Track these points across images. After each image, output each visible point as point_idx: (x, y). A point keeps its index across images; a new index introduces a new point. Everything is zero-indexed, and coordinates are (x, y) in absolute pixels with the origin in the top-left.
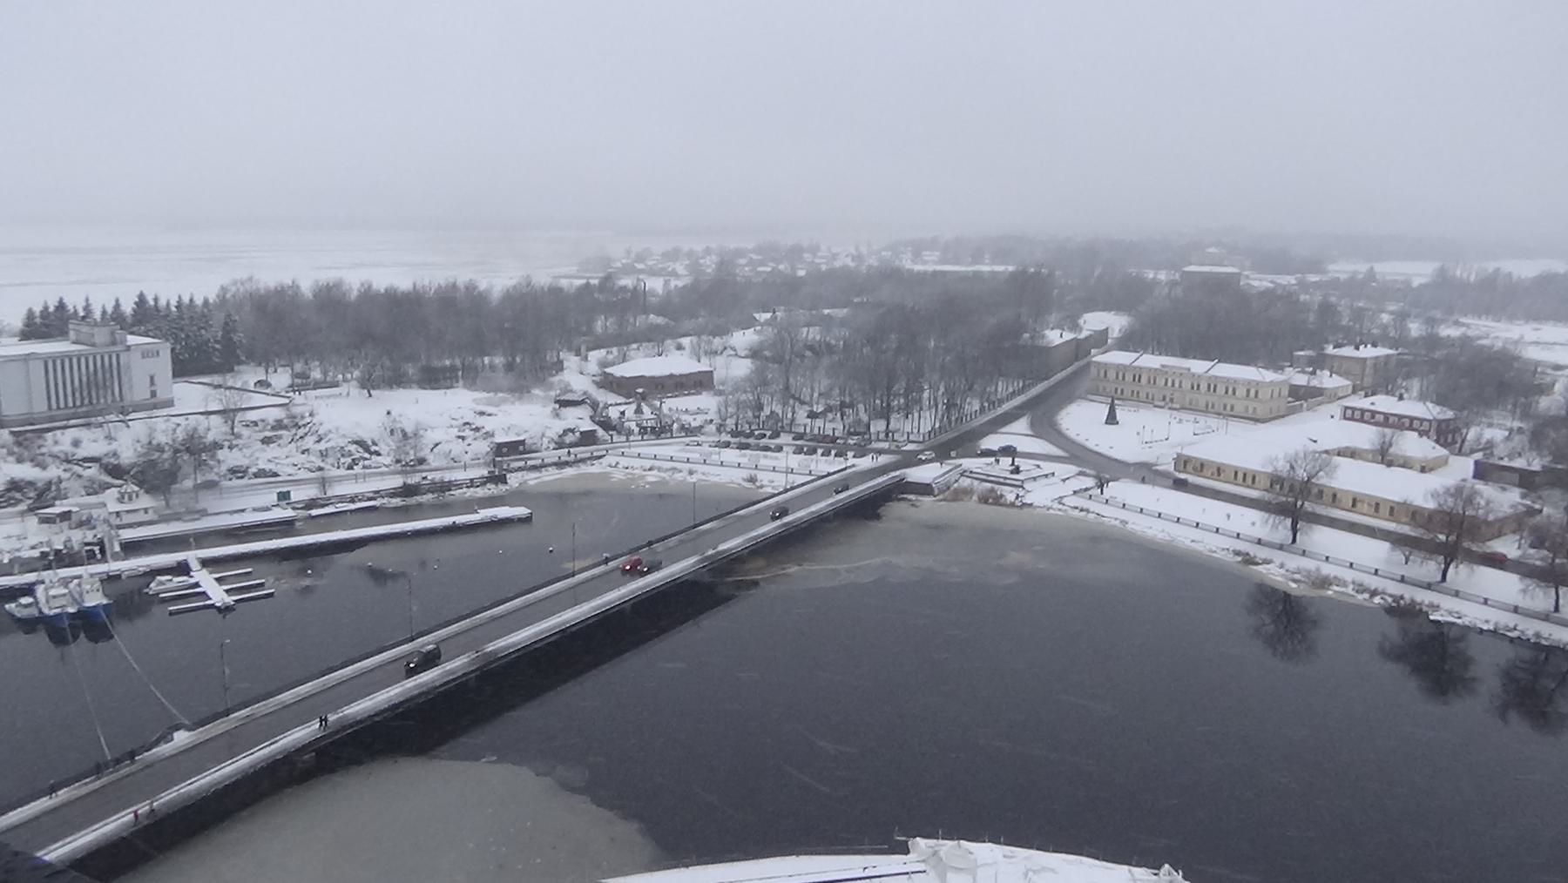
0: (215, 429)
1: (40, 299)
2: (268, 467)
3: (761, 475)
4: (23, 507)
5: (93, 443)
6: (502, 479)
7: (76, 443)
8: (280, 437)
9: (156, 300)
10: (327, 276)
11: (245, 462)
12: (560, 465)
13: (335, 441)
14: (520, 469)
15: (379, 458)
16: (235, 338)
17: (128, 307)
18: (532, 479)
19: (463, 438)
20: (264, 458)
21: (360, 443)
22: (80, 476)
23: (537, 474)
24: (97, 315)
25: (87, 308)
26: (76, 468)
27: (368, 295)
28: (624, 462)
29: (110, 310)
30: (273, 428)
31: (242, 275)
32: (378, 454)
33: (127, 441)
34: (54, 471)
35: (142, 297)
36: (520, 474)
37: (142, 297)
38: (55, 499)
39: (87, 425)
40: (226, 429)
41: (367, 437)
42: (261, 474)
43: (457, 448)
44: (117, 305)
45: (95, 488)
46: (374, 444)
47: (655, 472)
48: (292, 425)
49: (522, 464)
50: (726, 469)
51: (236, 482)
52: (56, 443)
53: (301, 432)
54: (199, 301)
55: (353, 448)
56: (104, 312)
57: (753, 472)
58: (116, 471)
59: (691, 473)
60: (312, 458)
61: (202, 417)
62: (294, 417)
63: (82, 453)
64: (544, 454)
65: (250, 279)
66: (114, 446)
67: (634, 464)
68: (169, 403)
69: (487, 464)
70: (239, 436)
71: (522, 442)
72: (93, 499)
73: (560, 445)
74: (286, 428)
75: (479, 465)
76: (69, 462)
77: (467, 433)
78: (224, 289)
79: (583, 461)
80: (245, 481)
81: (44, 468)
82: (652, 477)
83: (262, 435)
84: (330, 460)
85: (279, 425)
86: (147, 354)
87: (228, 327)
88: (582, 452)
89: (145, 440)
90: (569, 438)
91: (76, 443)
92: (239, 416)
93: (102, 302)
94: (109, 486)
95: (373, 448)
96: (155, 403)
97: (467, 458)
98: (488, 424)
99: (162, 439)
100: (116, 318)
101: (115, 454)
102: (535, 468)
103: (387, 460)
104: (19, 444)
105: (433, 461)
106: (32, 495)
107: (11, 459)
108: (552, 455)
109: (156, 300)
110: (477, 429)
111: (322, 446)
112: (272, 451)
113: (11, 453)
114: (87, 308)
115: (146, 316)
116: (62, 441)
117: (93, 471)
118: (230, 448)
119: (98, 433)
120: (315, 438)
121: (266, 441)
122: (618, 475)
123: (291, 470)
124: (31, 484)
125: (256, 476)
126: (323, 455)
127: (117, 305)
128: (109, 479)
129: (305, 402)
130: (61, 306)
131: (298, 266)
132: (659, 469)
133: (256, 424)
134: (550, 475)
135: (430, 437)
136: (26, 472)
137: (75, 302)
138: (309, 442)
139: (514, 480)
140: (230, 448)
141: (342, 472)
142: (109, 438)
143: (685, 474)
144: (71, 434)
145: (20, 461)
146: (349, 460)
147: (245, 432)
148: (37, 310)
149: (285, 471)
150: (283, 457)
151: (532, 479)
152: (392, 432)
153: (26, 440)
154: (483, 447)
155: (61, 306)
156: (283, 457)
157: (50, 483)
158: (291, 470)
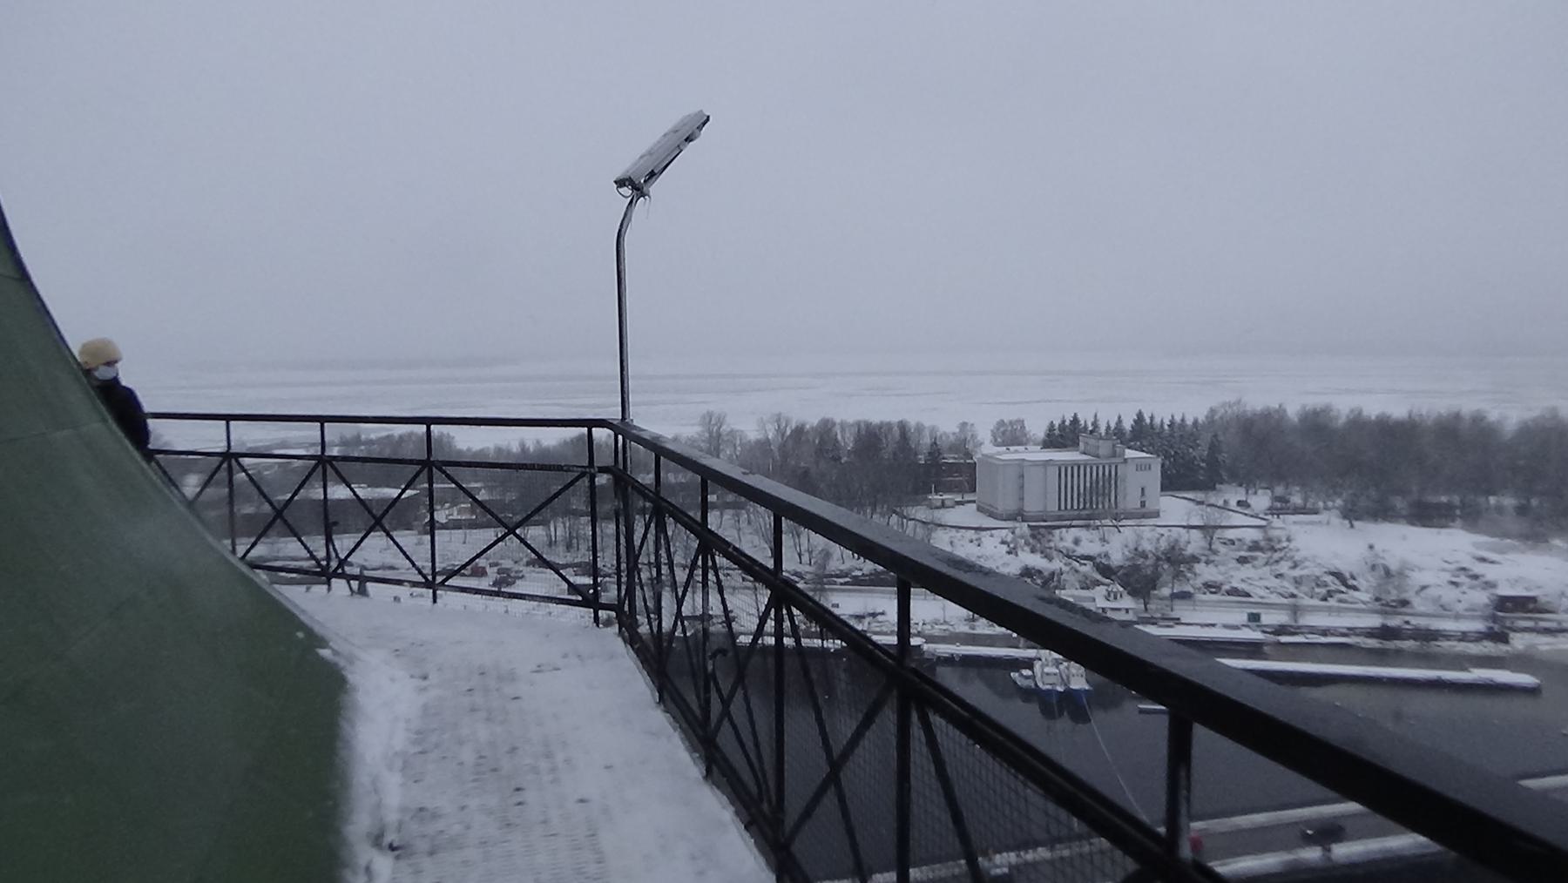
0: (1194, 543)
1: (1060, 414)
5: (1090, 543)
7: (1077, 542)
8: (1255, 558)
9: (1152, 418)
10: (1315, 402)
11: (1220, 578)
15: (1356, 594)
16: (1220, 458)
17: (1128, 424)
20: (1239, 577)
21: (1338, 575)
24: (1103, 430)
25: (1095, 424)
27: (1357, 423)
29: (1113, 425)
30: (1250, 549)
31: (1232, 398)
32: (1355, 588)
33: (1117, 545)
34: (1058, 564)
35: (1140, 415)
36: (1527, 636)
37: (1140, 415)
39: (1087, 527)
40: (1204, 544)
41: (1345, 569)
42: (1234, 592)
43: (1449, 595)
44: (1120, 421)
45: (1088, 584)
48: (1267, 548)
49: (1530, 624)
53: (1277, 556)
54: (1189, 422)
55: (1329, 579)
56: (1108, 427)
58: (1106, 571)
62: (1270, 540)
63: (1080, 551)
64: (1561, 616)
65: (1239, 402)
66: (1107, 548)
68: (1156, 514)
69: (1485, 618)
70: (1215, 553)
71: (1533, 599)
75: (1473, 618)
76: (1069, 557)
77: (1462, 579)
78: (1213, 411)
81: (1050, 559)
84: (1304, 588)
85: (1255, 546)
86: (1143, 467)
87: (1214, 448)
89: (1132, 546)
91: (1077, 542)
93: (1107, 418)
95: (1351, 582)
96: (1145, 513)
99: (1147, 546)
100: (1117, 433)
101: (1106, 555)
102: (1547, 631)
103: (1365, 597)
104: (1033, 536)
105: (1418, 604)
109: (1152, 418)
110: (1476, 577)
111: (1297, 573)
112: (1247, 571)
113: (1027, 544)
114: (1095, 424)
115: (1142, 433)
116: (1065, 538)
117: (1087, 568)
118: (1207, 563)
119: (1095, 535)
120: (1290, 564)
121: (1242, 561)
123: (1262, 592)
124: (1040, 572)
125: (1228, 593)
126: (1298, 582)
127: (1120, 421)
128: (1099, 577)
129: (1284, 526)
130: (1075, 420)
131: (1286, 391)
133: (1233, 543)
135: (1418, 578)
136: (1036, 561)
137: (1086, 418)
138: (1284, 568)
139: (1519, 642)
140: (1207, 563)
141: (1316, 602)
142: (1104, 540)
145: (1033, 551)
146: (1323, 591)
147: (1222, 549)
148: (1057, 423)
149: (1258, 592)
151: (1544, 644)
152: (1373, 567)
154: (1481, 598)
155: (1075, 420)
156: (1257, 579)
157: (1053, 574)
158: (1262, 592)
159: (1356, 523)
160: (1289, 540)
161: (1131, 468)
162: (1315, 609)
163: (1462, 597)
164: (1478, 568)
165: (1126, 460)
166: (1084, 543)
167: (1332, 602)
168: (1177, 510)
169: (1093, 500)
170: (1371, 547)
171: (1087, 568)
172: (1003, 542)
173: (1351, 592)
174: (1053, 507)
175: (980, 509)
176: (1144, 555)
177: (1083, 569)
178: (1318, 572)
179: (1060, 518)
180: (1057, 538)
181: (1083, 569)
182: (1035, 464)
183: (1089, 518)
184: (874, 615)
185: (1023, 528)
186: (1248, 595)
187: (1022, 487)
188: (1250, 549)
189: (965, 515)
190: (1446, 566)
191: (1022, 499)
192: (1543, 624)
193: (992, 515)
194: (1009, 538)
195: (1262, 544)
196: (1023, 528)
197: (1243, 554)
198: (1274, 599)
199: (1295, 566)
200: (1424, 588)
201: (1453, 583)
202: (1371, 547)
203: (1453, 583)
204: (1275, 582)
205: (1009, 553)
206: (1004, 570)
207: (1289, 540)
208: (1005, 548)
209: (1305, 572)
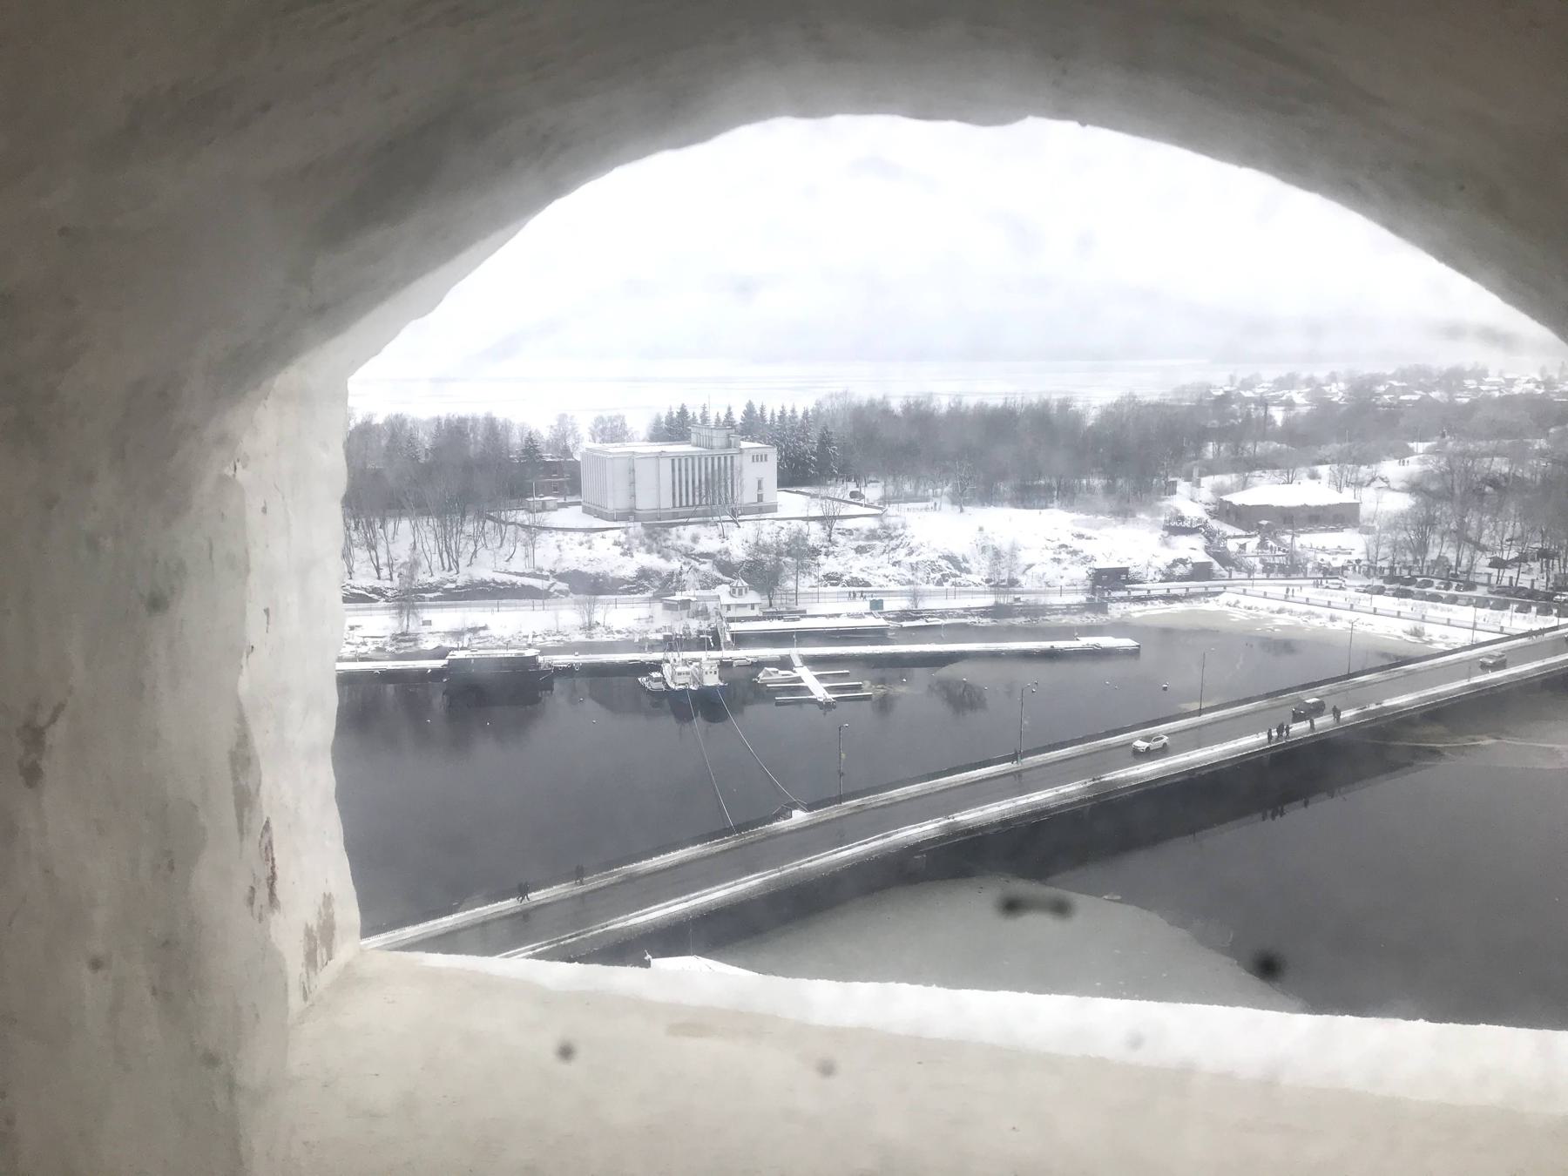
0: (815, 533)
2: (861, 576)
3: (1429, 629)
4: (649, 594)
5: (709, 540)
6: (1101, 608)
7: (695, 539)
8: (872, 547)
11: (840, 570)
12: (1169, 598)
13: (928, 555)
14: (1122, 599)
15: (969, 577)
18: (1136, 611)
19: (1058, 561)
20: (856, 566)
21: (951, 559)
22: (697, 570)
23: (1140, 607)
26: (693, 562)
28: (1246, 601)
30: (867, 538)
32: (969, 572)
33: (738, 541)
34: (675, 565)
36: (1122, 605)
38: (675, 589)
39: (705, 523)
40: (823, 535)
41: (958, 552)
42: (854, 582)
43: (1052, 572)
45: (708, 583)
46: (965, 560)
47: (1286, 615)
48: (885, 534)
49: (1125, 594)
50: (1386, 621)
51: (830, 589)
52: (679, 537)
53: (894, 543)
55: (943, 563)
57: (1419, 625)
58: (727, 568)
59: (1332, 619)
60: (902, 570)
61: (801, 523)
62: (885, 527)
63: (699, 548)
64: (1149, 586)
66: (726, 544)
67: (1253, 603)
68: (773, 508)
69: (1087, 591)
70: (834, 544)
71: (1125, 571)
72: (706, 593)
73: (1168, 577)
74: (879, 538)
75: (1076, 592)
76: (687, 555)
77: (1063, 556)
79: (1195, 596)
80: (839, 588)
81: (667, 558)
82: (1283, 620)
83: (855, 544)
84: (920, 574)
85: (872, 535)
86: (762, 458)
88: (1195, 586)
89: (752, 541)
90: (1180, 570)
91: (695, 539)
92: (838, 524)
94: (723, 582)
95: (964, 565)
96: (761, 508)
97: (1063, 582)
98: (1087, 548)
99: (767, 539)
101: (727, 552)
102: (1139, 600)
103: (977, 579)
104: (649, 536)
105: (1026, 582)
106: (657, 583)
107: (642, 549)
108: (1160, 589)
110: (1075, 553)
111: (913, 559)
112: (865, 561)
113: (642, 544)
116: (683, 535)
117: (707, 567)
118: (827, 555)
119: (714, 531)
120: (905, 551)
121: (860, 550)
122: (1239, 615)
123: (882, 581)
124: (658, 573)
125: (849, 584)
126: (914, 568)
128: (720, 575)
129: (897, 514)
132: (1291, 612)
133: (850, 532)
134: (1157, 609)
135: (1024, 558)
136: (654, 562)
138: (901, 554)
139: (1116, 611)
140: (827, 555)
141: (932, 587)
142: (723, 536)
143: (1325, 620)
144: (691, 529)
145: (649, 551)
146: (938, 576)
147: (841, 540)
149: (877, 581)
150: (875, 568)
151: (1136, 611)
152: (984, 549)
153: (656, 529)
154: (1080, 573)
156: (875, 568)
157: (672, 574)
158: (882, 581)
159: (968, 509)
160: (904, 527)
161: (747, 459)
162: (931, 594)
163: (1064, 573)
164: (1077, 544)
165: (741, 451)
166: (703, 540)
167: (947, 585)
168: (794, 503)
169: (709, 494)
170: (981, 529)
171: (707, 567)
172: (616, 544)
173: (964, 575)
174: (667, 503)
175: (587, 511)
176: (765, 549)
177: (703, 568)
178: (933, 556)
179: (675, 515)
180: (673, 537)
181: (703, 568)
182: (646, 457)
183: (705, 514)
184: (474, 630)
185: (636, 528)
186: (867, 584)
187: (633, 483)
188: (867, 538)
189: (570, 516)
190: (1050, 544)
191: (634, 496)
192: (1134, 593)
193: (600, 516)
194: (623, 538)
195: (880, 532)
196: (636, 528)
197: (862, 543)
198: (893, 587)
199: (911, 553)
200: (1030, 566)
201: (1054, 560)
202: (981, 529)
203: (1054, 560)
204: (891, 571)
205: (623, 554)
206: (622, 573)
207: (904, 527)
208: (618, 550)
209: (920, 558)
